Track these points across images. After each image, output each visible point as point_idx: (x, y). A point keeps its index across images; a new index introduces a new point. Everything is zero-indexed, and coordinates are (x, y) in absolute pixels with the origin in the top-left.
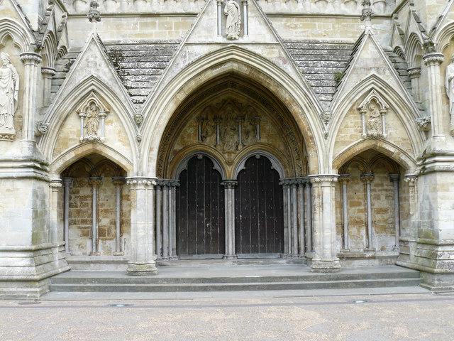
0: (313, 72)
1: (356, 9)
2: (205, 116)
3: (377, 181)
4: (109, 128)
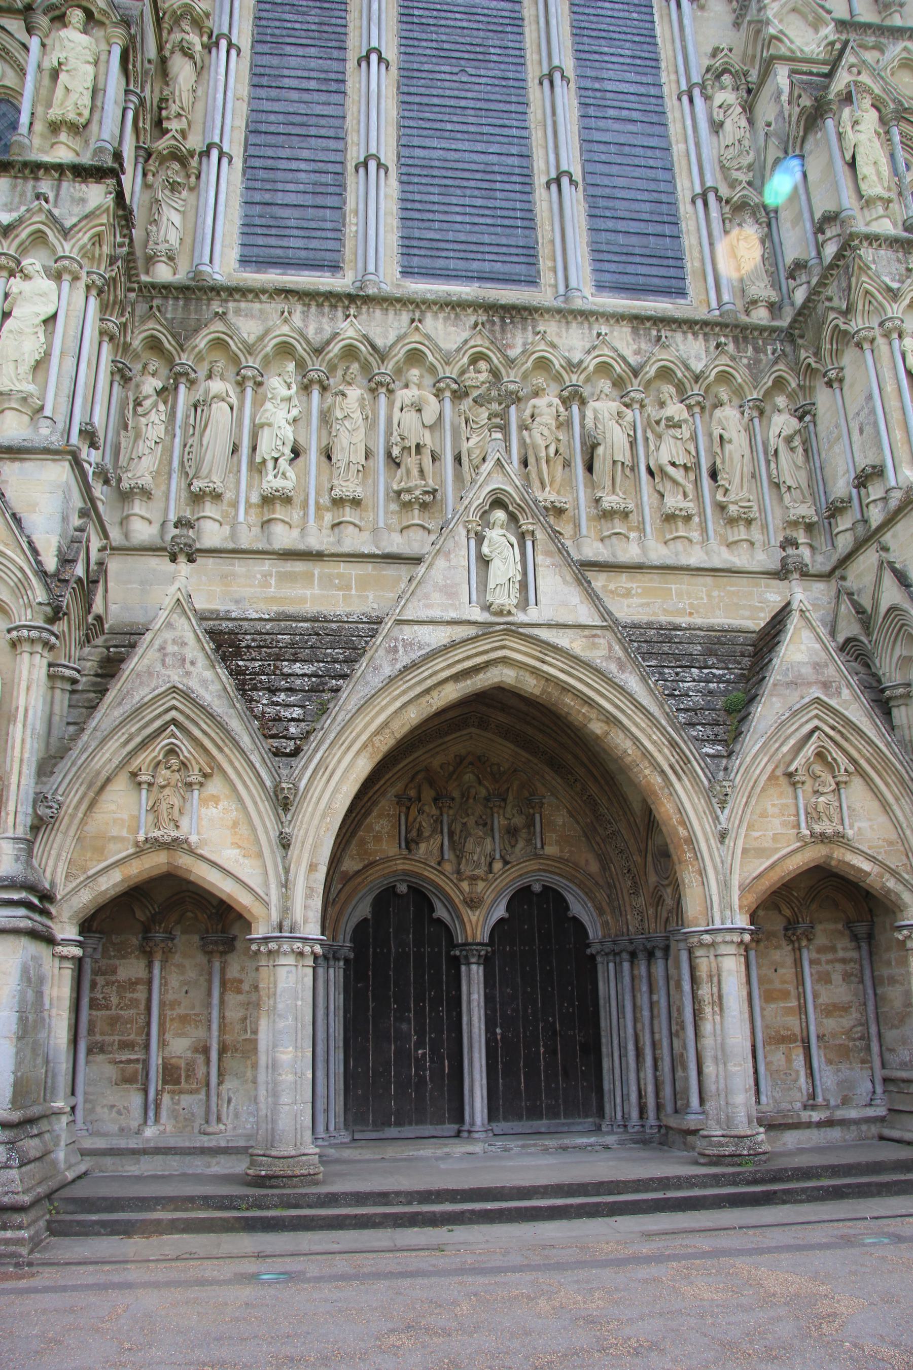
0: (677, 693)
1: (752, 557)
2: (412, 793)
3: (821, 939)
4: (212, 812)
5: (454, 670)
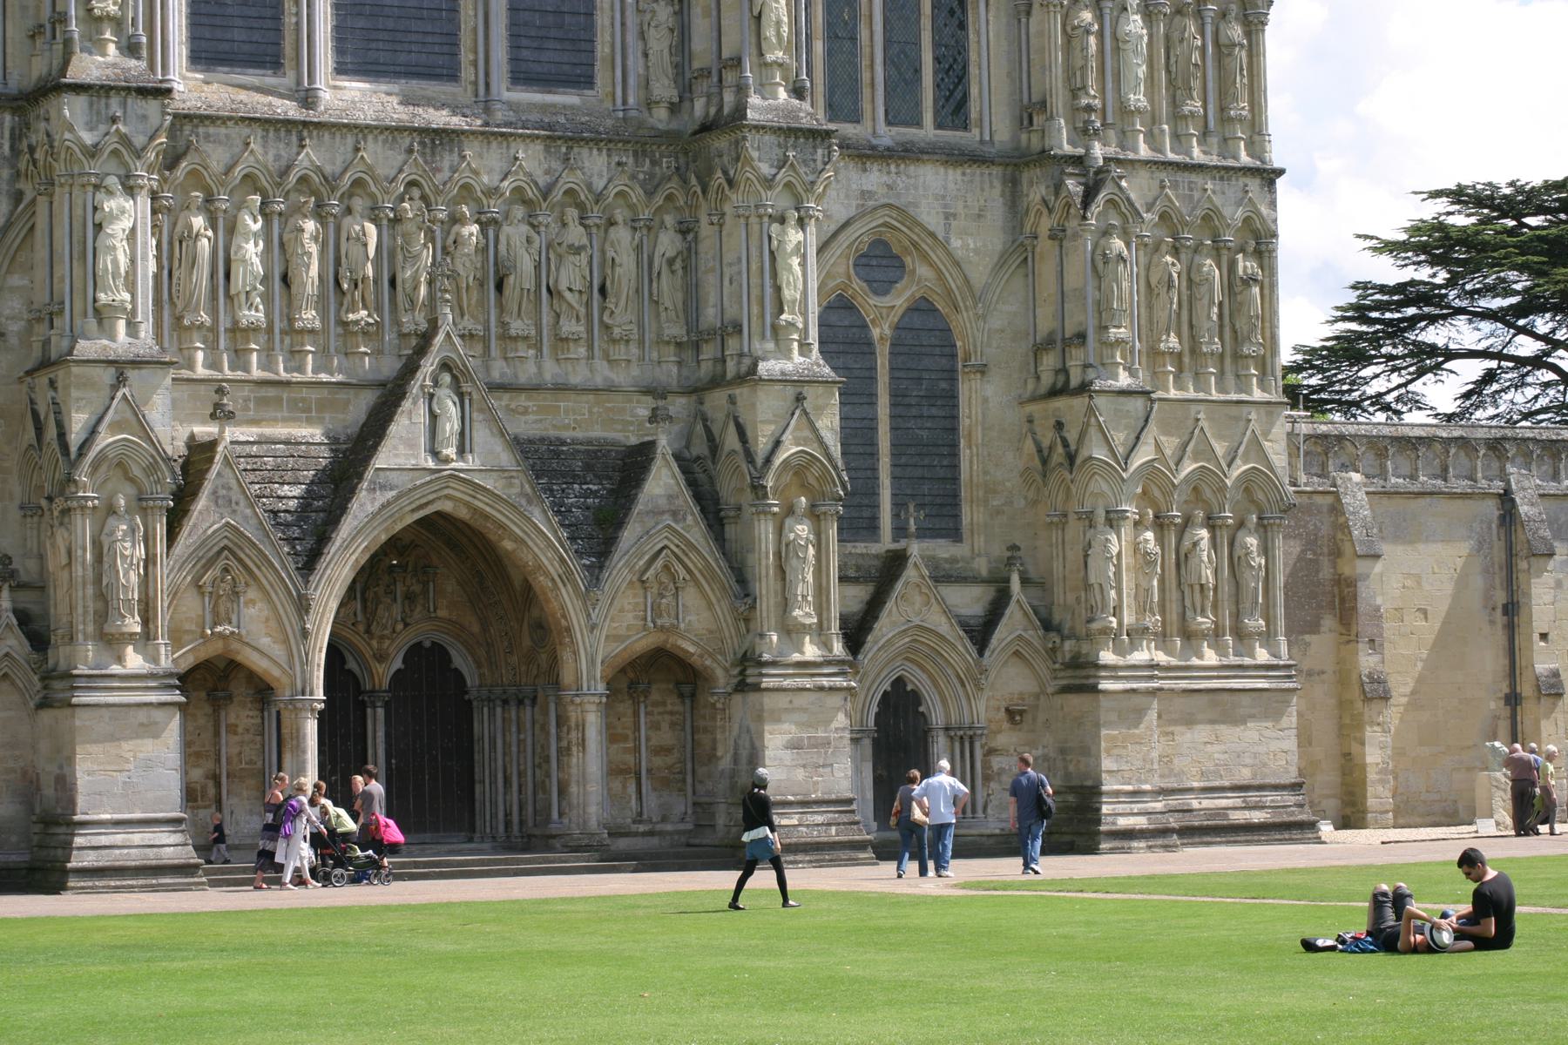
3: (655, 696)
4: (252, 611)
5: (414, 506)
